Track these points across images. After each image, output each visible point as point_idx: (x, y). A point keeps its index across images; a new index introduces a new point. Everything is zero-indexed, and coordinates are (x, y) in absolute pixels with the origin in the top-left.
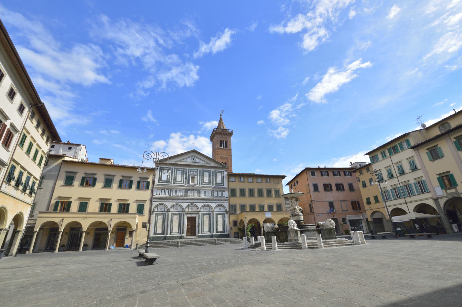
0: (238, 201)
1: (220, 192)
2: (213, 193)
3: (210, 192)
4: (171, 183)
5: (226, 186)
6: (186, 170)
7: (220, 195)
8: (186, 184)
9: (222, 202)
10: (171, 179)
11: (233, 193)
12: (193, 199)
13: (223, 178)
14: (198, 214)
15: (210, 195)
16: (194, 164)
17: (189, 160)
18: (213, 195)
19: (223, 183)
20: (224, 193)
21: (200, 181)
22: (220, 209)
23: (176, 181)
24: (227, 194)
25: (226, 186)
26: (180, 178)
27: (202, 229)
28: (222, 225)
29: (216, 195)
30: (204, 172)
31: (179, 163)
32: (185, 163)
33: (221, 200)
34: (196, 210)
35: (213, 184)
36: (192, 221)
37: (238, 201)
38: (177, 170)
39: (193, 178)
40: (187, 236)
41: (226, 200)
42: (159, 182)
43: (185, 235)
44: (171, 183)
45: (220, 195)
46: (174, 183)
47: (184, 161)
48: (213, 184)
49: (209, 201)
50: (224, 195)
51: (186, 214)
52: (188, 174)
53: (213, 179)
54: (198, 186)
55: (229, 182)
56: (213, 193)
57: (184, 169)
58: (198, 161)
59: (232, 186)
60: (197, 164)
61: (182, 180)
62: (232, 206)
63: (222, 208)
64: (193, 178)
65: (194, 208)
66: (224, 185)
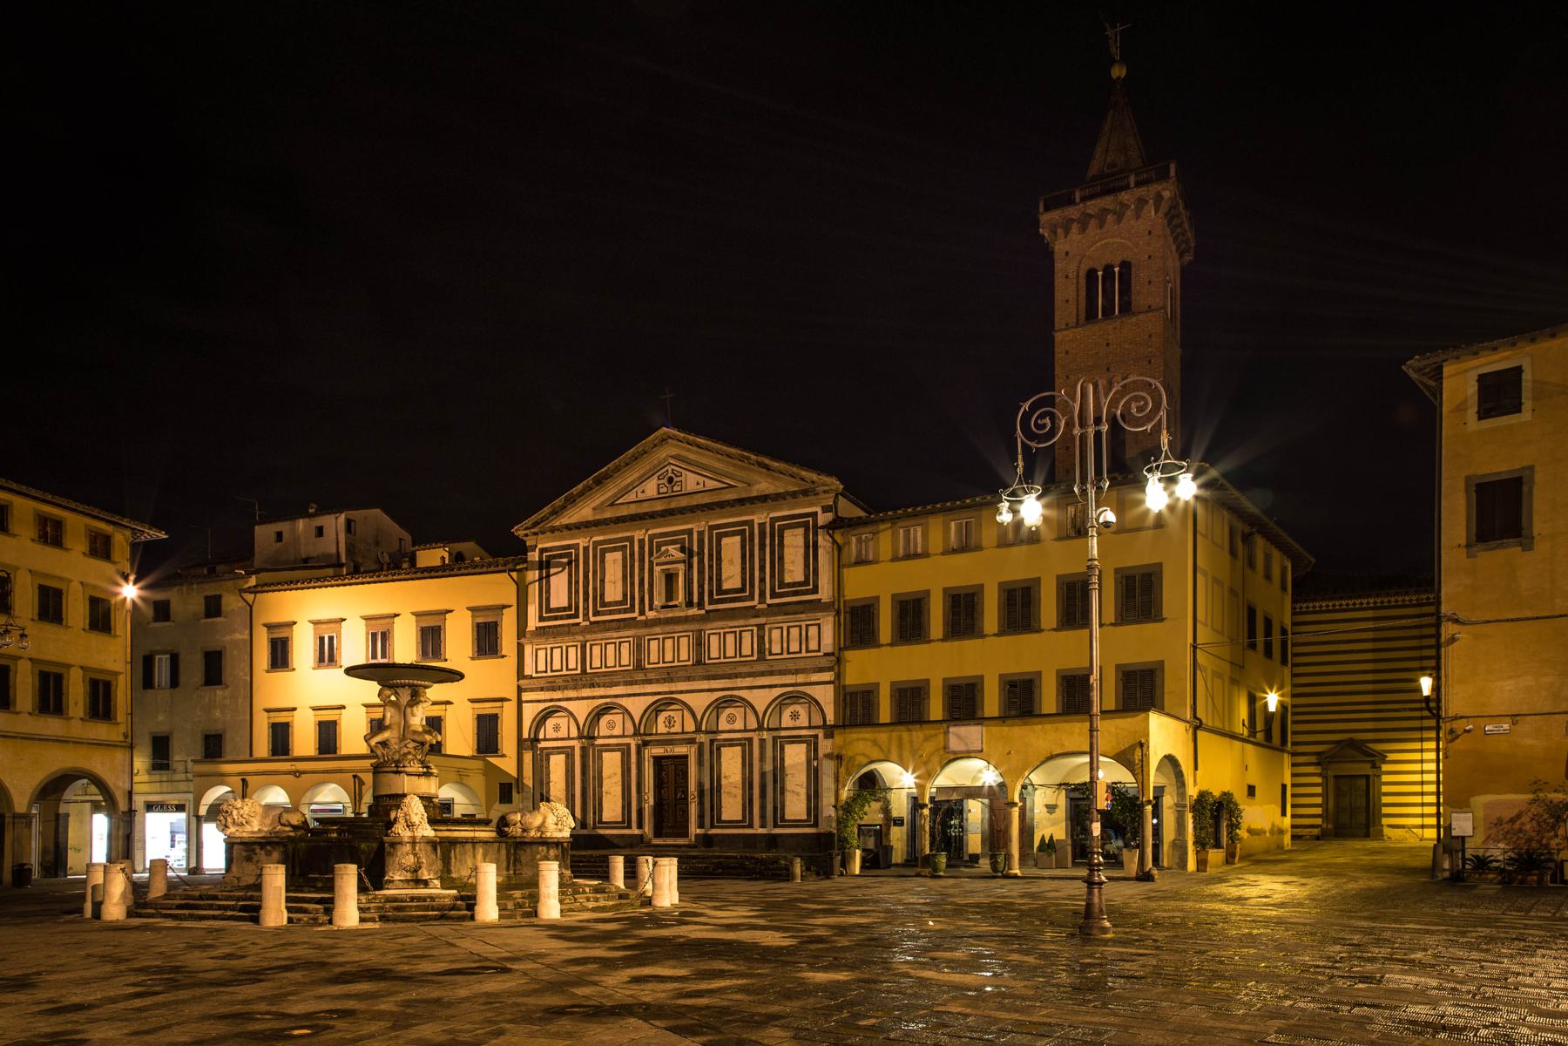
0: (882, 667)
1: (795, 632)
2: (761, 638)
3: (747, 637)
4: (586, 615)
5: (825, 593)
6: (641, 542)
7: (794, 647)
8: (642, 612)
9: (801, 678)
10: (586, 600)
11: (858, 625)
12: (669, 675)
13: (811, 550)
14: (691, 741)
15: (746, 650)
16: (673, 505)
17: (651, 488)
18: (761, 651)
19: (810, 581)
20: (813, 631)
21: (701, 586)
22: (795, 716)
23: (604, 604)
24: (826, 633)
25: (825, 593)
26: (620, 584)
27: (716, 807)
28: (803, 791)
29: (776, 649)
30: (720, 537)
31: (608, 515)
32: (633, 510)
33: (797, 672)
34: (690, 726)
35: (762, 594)
36: (670, 772)
37: (882, 667)
38: (604, 552)
39: (670, 578)
40: (658, 834)
41: (821, 670)
42: (541, 619)
43: (648, 829)
44: (586, 615)
45: (794, 647)
46: (596, 613)
47: (631, 497)
48: (762, 594)
49: (739, 682)
50: (813, 645)
51: (646, 744)
52: (651, 563)
53: (762, 569)
54: (694, 611)
55: (839, 566)
56: (761, 638)
57: (631, 540)
58: (691, 481)
59: (859, 584)
60: (684, 502)
61: (625, 595)
62: (853, 694)
63: (802, 710)
64: (670, 578)
65: (677, 716)
66: (815, 590)
